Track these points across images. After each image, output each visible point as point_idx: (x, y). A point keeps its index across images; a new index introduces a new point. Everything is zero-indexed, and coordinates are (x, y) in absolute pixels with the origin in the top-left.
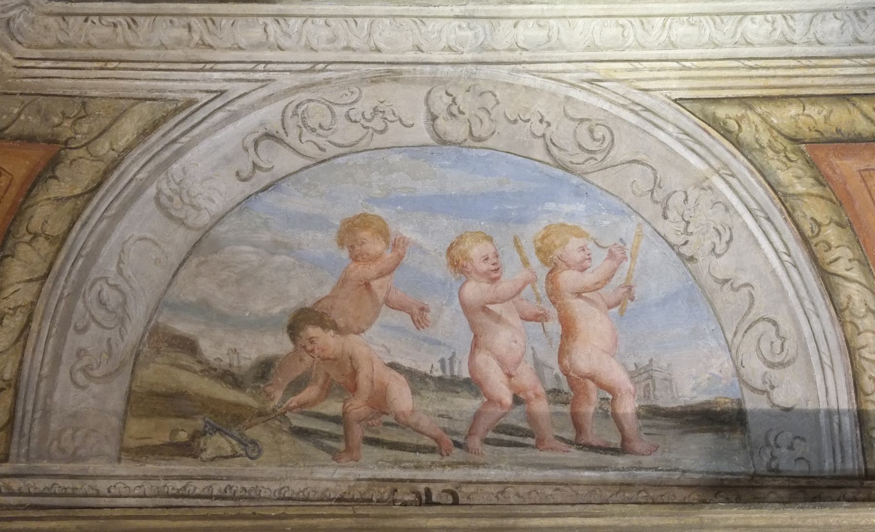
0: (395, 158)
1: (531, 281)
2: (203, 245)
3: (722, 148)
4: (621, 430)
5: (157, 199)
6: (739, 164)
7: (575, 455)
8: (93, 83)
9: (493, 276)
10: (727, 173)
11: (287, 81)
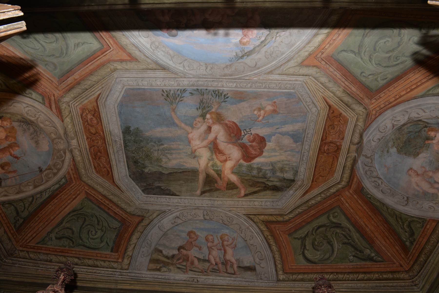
0: (197, 221)
1: (219, 243)
2: (165, 234)
3: (251, 222)
4: (234, 270)
5: (158, 227)
6: (254, 225)
7: (226, 274)
8: (150, 208)
9: (213, 242)
10: (252, 226)
11: (181, 208)
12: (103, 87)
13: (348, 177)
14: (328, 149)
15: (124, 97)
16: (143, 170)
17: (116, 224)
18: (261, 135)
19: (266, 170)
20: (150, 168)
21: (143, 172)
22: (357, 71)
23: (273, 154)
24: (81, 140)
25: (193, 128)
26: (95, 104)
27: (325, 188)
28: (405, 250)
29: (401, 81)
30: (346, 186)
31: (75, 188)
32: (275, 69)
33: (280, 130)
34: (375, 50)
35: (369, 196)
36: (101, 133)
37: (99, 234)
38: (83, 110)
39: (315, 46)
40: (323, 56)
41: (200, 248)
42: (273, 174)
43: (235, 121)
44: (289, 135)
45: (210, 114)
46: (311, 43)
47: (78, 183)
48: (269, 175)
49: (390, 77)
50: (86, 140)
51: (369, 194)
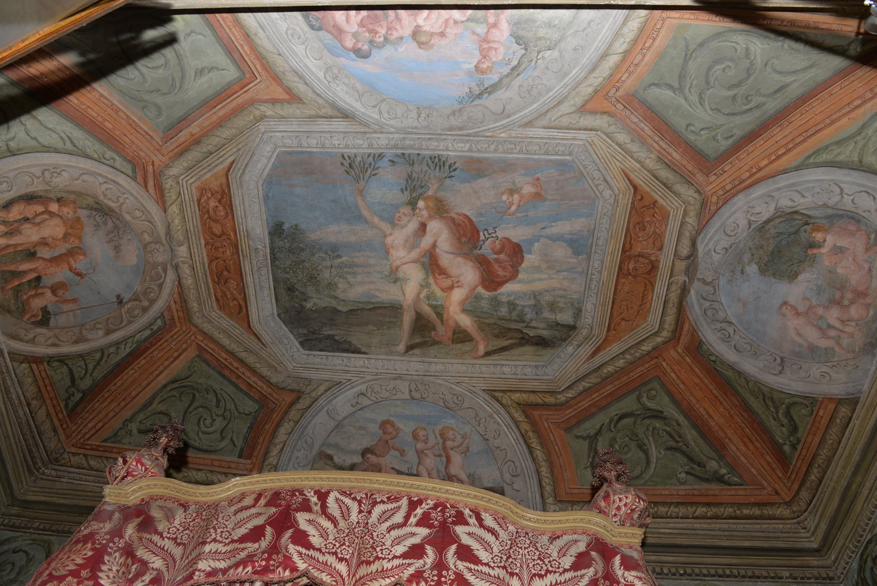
8: (314, 375)
11: (369, 377)
12: (239, 150)
13: (673, 322)
14: (635, 269)
15: (274, 167)
16: (304, 303)
17: (249, 406)
18: (515, 240)
19: (524, 306)
20: (315, 300)
21: (303, 307)
22: (680, 123)
23: (537, 276)
24: (195, 246)
25: (394, 225)
26: (224, 180)
27: (632, 342)
28: (783, 460)
29: (759, 141)
30: (670, 340)
31: (180, 338)
32: (537, 118)
33: (548, 231)
34: (707, 83)
35: (713, 358)
36: (232, 234)
37: (219, 424)
38: (202, 191)
39: (604, 75)
40: (618, 94)
41: (402, 453)
42: (537, 313)
43: (468, 214)
44: (565, 241)
45: (425, 199)
46: (597, 71)
47: (184, 328)
48: (529, 316)
49: (738, 133)
50: (203, 246)
51: (712, 354)
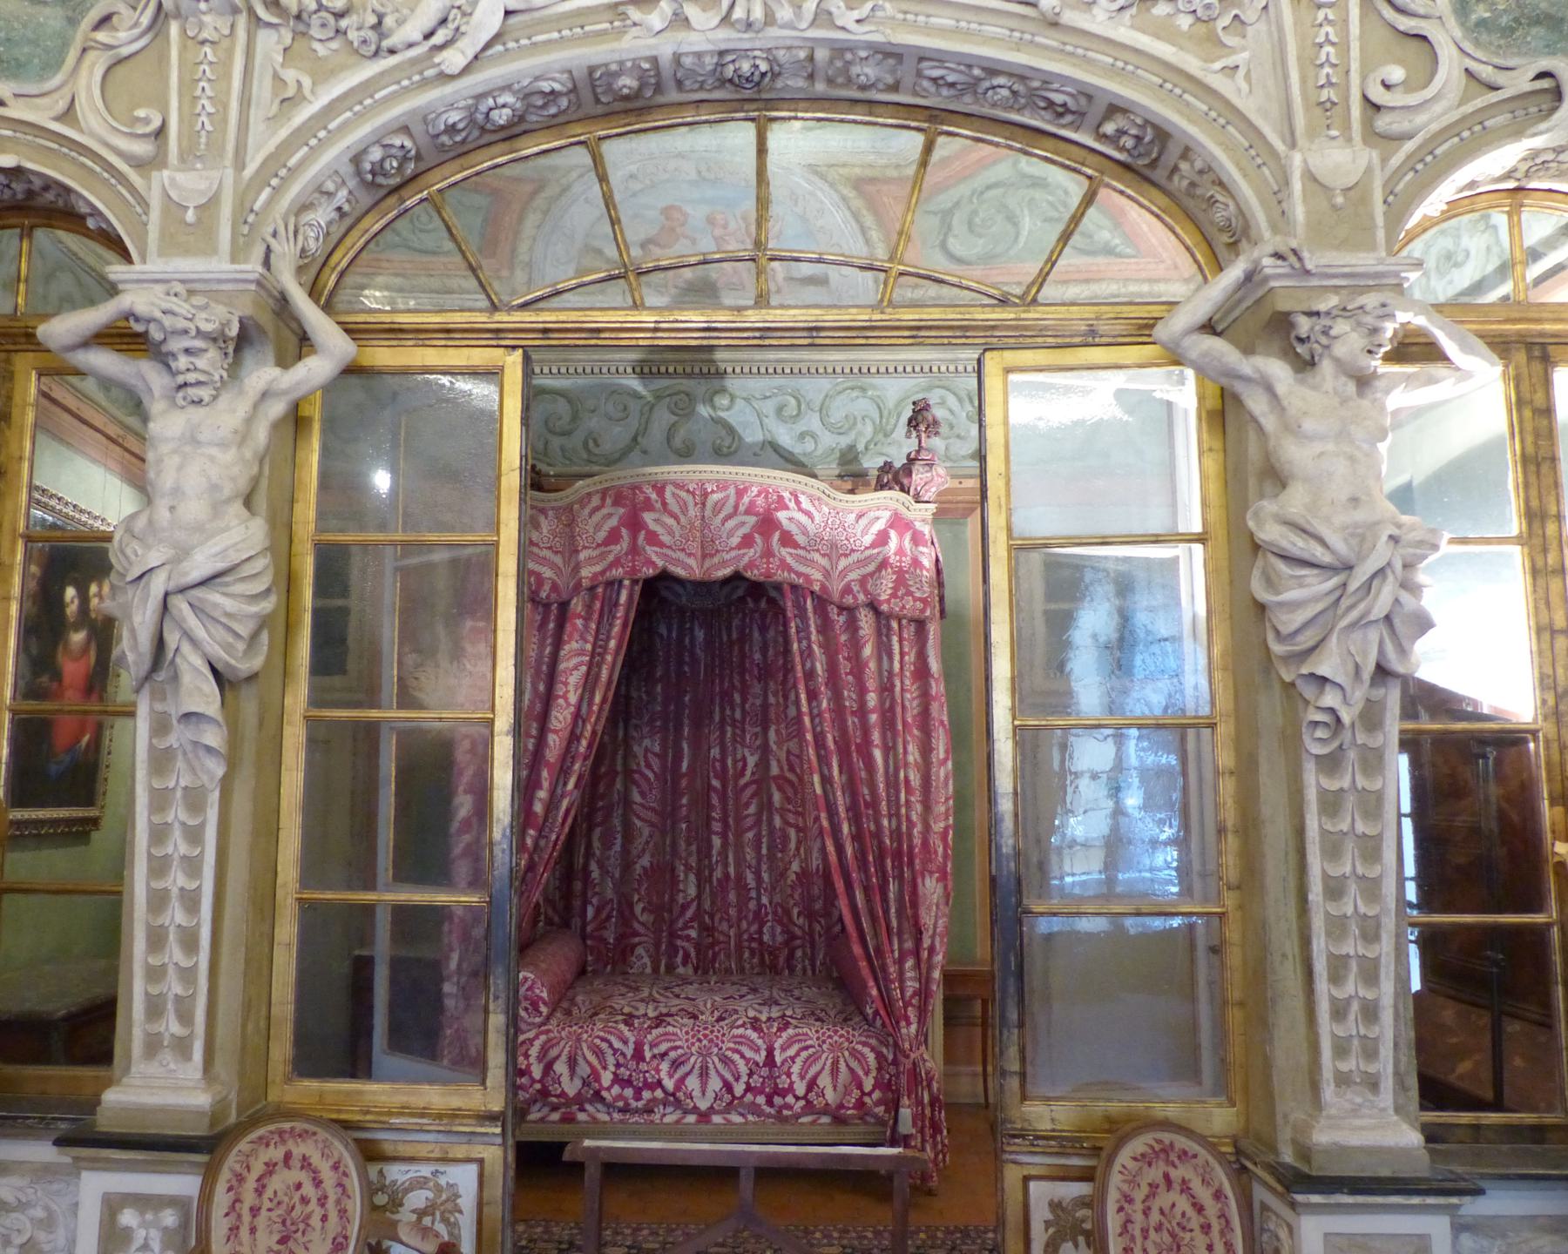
9: (725, 227)
